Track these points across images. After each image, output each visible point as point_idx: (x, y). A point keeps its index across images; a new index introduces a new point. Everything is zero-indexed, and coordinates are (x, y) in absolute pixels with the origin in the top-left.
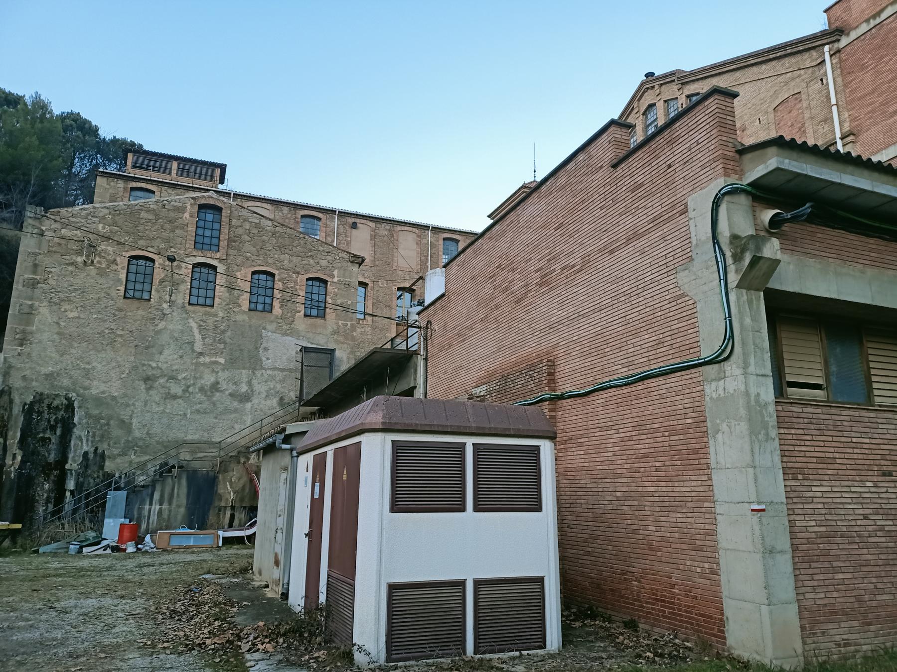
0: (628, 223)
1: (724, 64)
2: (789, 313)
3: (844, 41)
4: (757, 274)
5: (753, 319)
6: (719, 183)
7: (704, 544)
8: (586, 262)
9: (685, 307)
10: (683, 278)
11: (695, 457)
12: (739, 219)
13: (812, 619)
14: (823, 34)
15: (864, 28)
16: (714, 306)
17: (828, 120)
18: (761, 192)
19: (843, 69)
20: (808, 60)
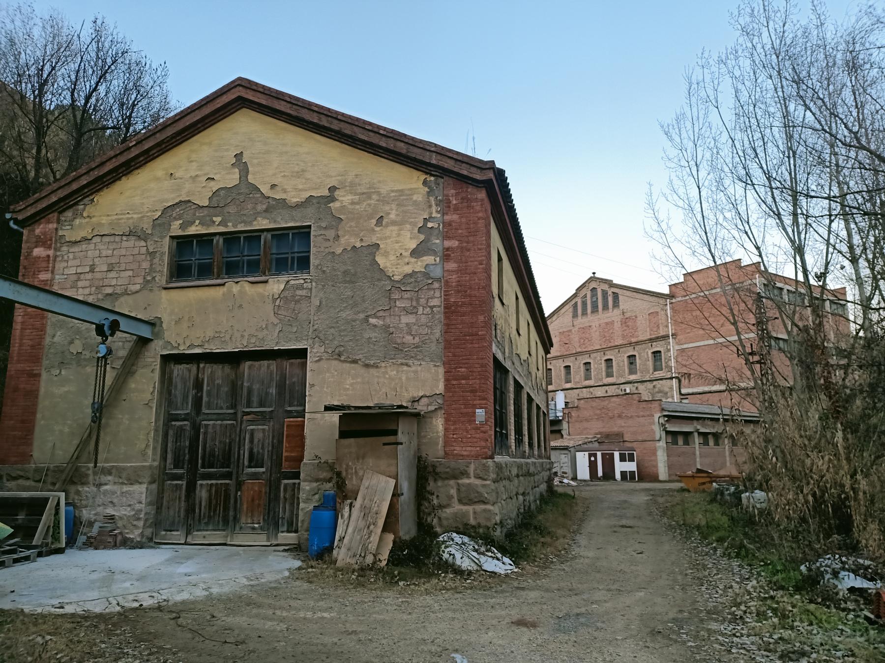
0: (642, 413)
1: (630, 287)
2: (668, 433)
3: (674, 301)
4: (665, 429)
5: (664, 434)
6: (659, 415)
7: (656, 466)
8: (631, 417)
9: (654, 433)
10: (653, 427)
11: (654, 452)
12: (662, 421)
13: (670, 475)
14: (667, 295)
15: (680, 299)
16: (658, 432)
17: (667, 326)
18: (665, 416)
19: (672, 309)
20: (662, 301)
